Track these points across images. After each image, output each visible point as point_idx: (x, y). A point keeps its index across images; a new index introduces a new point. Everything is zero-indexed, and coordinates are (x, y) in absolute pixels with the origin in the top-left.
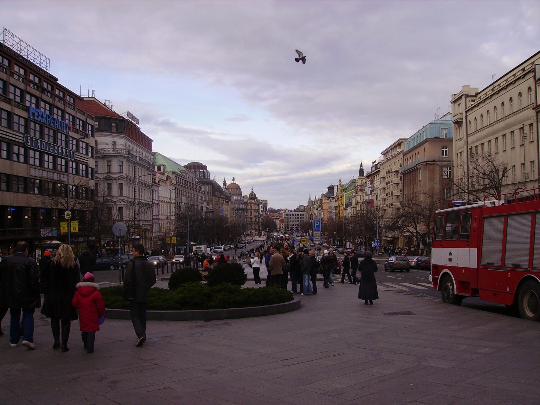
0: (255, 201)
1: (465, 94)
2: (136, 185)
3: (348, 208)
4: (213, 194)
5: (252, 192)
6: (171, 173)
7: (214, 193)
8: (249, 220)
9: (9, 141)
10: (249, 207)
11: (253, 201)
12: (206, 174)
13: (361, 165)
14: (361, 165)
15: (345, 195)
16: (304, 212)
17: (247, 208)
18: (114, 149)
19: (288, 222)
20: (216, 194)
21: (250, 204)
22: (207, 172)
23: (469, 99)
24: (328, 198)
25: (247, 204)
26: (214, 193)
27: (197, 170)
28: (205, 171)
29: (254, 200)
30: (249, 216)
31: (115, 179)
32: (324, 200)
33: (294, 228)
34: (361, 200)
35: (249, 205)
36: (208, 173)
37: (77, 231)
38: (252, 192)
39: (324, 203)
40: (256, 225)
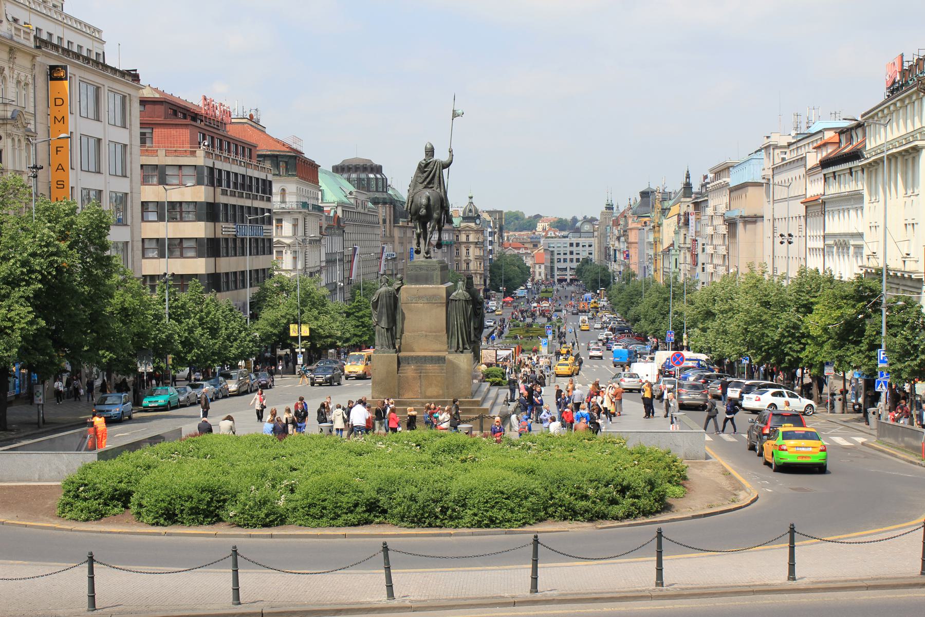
1: (773, 145)
2: (308, 248)
4: (394, 223)
6: (334, 205)
7: (396, 221)
8: (464, 266)
9: (227, 237)
10: (463, 238)
11: (473, 225)
12: (380, 184)
13: (688, 177)
14: (688, 177)
16: (593, 239)
17: (458, 240)
18: (283, 202)
19: (552, 262)
20: (401, 224)
21: (466, 231)
22: (383, 179)
23: (777, 151)
25: (459, 231)
26: (396, 221)
27: (363, 176)
28: (378, 176)
29: (475, 222)
30: (464, 258)
31: (289, 246)
33: (568, 278)
34: (685, 243)
35: (464, 232)
36: (385, 181)
37: (307, 334)
38: (472, 203)
39: (631, 229)
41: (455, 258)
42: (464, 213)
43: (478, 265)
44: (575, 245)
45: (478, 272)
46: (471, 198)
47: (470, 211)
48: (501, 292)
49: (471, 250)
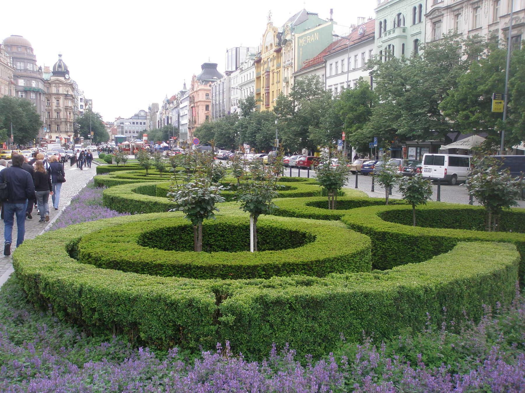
0: (65, 78)
3: (326, 62)
5: (60, 60)
8: (55, 115)
11: (62, 79)
15: (298, 38)
21: (56, 83)
24: (206, 82)
25: (49, 83)
29: (65, 77)
30: (54, 108)
32: (196, 86)
35: (54, 85)
38: (60, 60)
39: (197, 91)
40: (68, 125)
41: (46, 108)
42: (54, 68)
43: (68, 114)
44: (135, 123)
45: (68, 120)
46: (60, 56)
47: (60, 66)
48: (89, 139)
49: (61, 101)
